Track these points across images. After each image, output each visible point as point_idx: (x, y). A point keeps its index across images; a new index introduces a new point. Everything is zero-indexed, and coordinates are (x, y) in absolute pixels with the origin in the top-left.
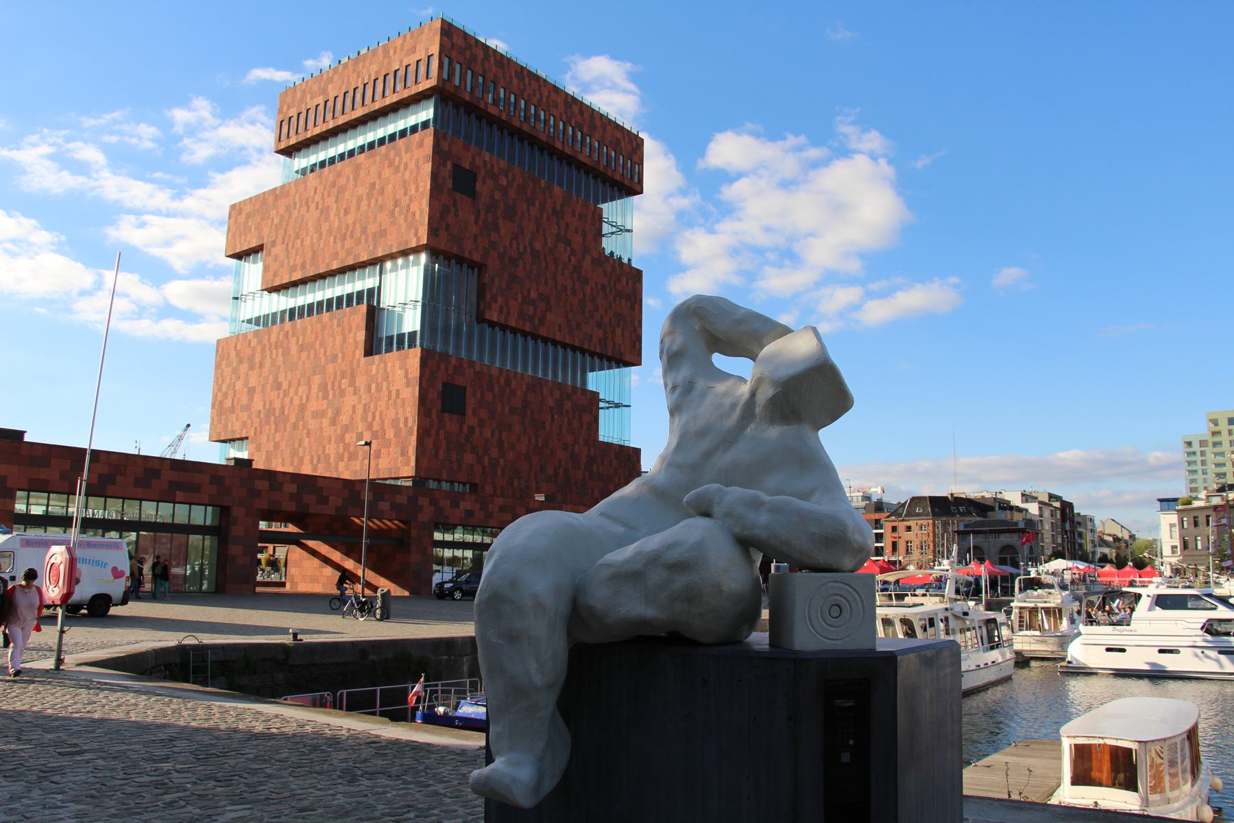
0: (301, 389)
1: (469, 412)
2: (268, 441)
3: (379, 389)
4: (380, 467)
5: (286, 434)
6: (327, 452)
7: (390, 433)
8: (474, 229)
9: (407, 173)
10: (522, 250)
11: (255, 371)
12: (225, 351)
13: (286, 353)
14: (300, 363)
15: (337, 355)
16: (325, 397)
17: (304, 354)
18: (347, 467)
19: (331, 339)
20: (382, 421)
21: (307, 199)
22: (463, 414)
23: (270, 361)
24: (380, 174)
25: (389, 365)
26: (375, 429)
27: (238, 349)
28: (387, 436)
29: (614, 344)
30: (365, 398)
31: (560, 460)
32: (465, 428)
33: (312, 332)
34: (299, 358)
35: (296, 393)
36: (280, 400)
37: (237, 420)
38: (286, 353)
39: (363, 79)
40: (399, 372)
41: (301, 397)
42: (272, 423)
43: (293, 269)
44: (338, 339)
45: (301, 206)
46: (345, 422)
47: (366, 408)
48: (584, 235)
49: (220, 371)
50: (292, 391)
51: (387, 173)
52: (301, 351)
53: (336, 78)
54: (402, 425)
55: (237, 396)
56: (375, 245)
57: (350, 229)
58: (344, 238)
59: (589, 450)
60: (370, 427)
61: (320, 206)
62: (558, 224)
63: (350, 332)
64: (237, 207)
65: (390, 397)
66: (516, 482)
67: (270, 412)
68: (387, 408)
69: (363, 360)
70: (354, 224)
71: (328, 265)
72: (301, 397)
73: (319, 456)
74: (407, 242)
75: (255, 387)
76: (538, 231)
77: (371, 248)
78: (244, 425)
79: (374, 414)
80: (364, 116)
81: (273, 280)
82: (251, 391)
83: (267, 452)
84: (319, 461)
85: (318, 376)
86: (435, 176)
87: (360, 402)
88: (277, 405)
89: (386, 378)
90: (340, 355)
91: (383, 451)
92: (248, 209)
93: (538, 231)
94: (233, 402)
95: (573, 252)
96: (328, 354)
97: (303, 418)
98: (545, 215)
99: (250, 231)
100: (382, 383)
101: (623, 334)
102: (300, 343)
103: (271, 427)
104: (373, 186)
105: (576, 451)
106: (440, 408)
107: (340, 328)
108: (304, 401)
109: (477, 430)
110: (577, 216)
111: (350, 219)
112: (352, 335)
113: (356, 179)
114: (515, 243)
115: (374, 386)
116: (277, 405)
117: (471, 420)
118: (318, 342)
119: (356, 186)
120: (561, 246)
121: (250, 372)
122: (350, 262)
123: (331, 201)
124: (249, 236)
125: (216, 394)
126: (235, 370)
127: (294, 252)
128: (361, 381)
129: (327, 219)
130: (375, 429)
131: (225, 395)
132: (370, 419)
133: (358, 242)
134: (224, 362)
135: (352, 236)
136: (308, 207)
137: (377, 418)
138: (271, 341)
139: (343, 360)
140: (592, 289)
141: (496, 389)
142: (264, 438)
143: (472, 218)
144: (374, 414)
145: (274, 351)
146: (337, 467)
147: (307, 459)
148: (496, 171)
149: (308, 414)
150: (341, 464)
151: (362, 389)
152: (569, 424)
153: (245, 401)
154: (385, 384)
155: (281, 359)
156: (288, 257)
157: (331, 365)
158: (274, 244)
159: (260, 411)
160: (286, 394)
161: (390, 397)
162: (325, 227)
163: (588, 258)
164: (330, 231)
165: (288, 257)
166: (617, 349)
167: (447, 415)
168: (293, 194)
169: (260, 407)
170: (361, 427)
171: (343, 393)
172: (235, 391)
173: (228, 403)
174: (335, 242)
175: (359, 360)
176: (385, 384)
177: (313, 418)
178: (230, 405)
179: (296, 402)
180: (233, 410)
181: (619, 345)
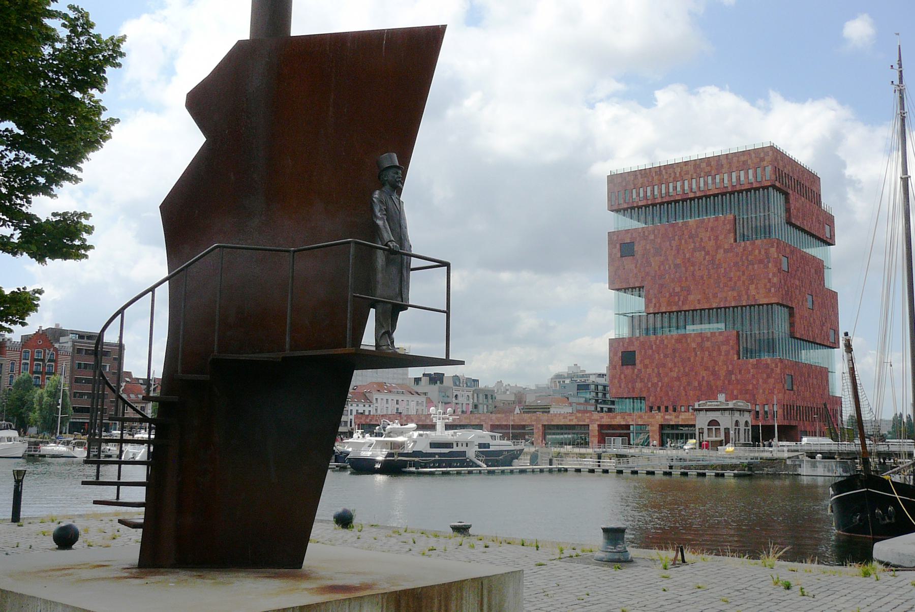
1: (638, 361)
10: (667, 268)
22: (634, 364)
29: (748, 296)
31: (703, 377)
32: (636, 370)
48: (717, 238)
59: (728, 367)
62: (694, 242)
66: (670, 393)
76: (678, 252)
86: (610, 255)
93: (678, 252)
95: (708, 253)
98: (683, 241)
101: (756, 288)
105: (716, 369)
106: (621, 364)
109: (643, 370)
110: (709, 229)
114: (662, 268)
117: (639, 366)
120: (697, 254)
140: (725, 269)
141: (654, 347)
148: (646, 234)
152: (709, 355)
166: (751, 298)
167: (625, 367)
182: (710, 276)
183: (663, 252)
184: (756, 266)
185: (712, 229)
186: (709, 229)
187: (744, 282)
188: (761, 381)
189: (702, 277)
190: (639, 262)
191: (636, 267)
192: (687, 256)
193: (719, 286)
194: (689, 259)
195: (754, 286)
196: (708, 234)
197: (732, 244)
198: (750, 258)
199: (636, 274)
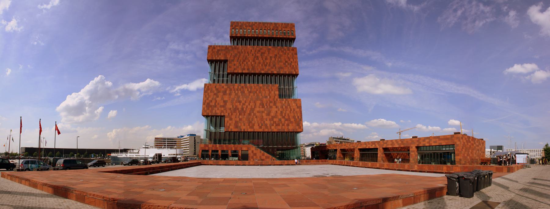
0: (251, 104)
2: (236, 118)
3: (286, 107)
4: (289, 128)
5: (245, 117)
6: (266, 123)
7: (292, 120)
9: (289, 56)
11: (227, 96)
12: (210, 87)
13: (243, 92)
14: (250, 96)
15: (267, 96)
16: (263, 107)
17: (252, 94)
18: (275, 128)
19: (264, 92)
20: (289, 117)
21: (248, 53)
23: (234, 94)
24: (278, 54)
25: (290, 102)
26: (286, 118)
27: (217, 88)
28: (291, 120)
30: (280, 110)
33: (255, 88)
34: (249, 95)
35: (249, 105)
36: (241, 106)
37: (218, 109)
38: (243, 92)
39: (267, 28)
40: (294, 104)
41: (252, 106)
42: (237, 112)
43: (244, 69)
44: (267, 92)
45: (245, 53)
46: (273, 115)
47: (281, 112)
49: (207, 94)
50: (247, 104)
51: (281, 53)
52: (251, 93)
53: (256, 25)
54: (297, 117)
55: (217, 102)
56: (279, 70)
57: (268, 64)
58: (266, 66)
60: (284, 117)
61: (254, 55)
63: (272, 90)
64: (213, 47)
65: (291, 110)
67: (236, 109)
68: (290, 112)
69: (279, 99)
70: (270, 63)
71: (260, 71)
72: (252, 106)
73: (261, 124)
74: (292, 72)
75: (227, 101)
77: (278, 70)
78: (222, 111)
79: (285, 114)
80: (268, 37)
81: (234, 71)
82: (225, 102)
83: (235, 121)
84: (262, 125)
85: (259, 101)
87: (279, 110)
88: (240, 107)
89: (289, 105)
90: (268, 97)
91: (290, 124)
92: (219, 48)
94: (215, 104)
96: (263, 95)
97: (253, 112)
99: (220, 54)
100: (287, 106)
102: (249, 90)
103: (237, 114)
104: (276, 55)
107: (268, 89)
108: (253, 107)
111: (268, 61)
112: (273, 92)
113: (269, 52)
115: (284, 107)
116: (240, 107)
118: (258, 92)
119: (269, 54)
121: (224, 96)
122: (270, 72)
123: (259, 55)
124: (220, 56)
125: (205, 101)
126: (215, 94)
127: (243, 65)
128: (279, 105)
129: (258, 59)
130: (286, 118)
131: (211, 101)
132: (284, 115)
133: (272, 68)
134: (209, 91)
135: (269, 66)
136: (248, 54)
137: (287, 115)
138: (235, 88)
139: (270, 97)
142: (233, 117)
144: (285, 114)
145: (236, 92)
146: (271, 128)
147: (256, 125)
149: (255, 112)
150: (273, 127)
151: (279, 107)
153: (222, 104)
154: (289, 107)
155: (240, 94)
156: (240, 65)
157: (264, 99)
158: (233, 61)
159: (231, 108)
160: (244, 104)
161: (291, 110)
162: (257, 61)
164: (260, 63)
165: (240, 65)
168: (241, 49)
169: (231, 107)
170: (280, 117)
171: (271, 107)
172: (216, 101)
173: (213, 104)
174: (262, 65)
175: (277, 99)
176: (289, 107)
177: (257, 113)
178: (214, 104)
179: (249, 107)
180: (216, 106)
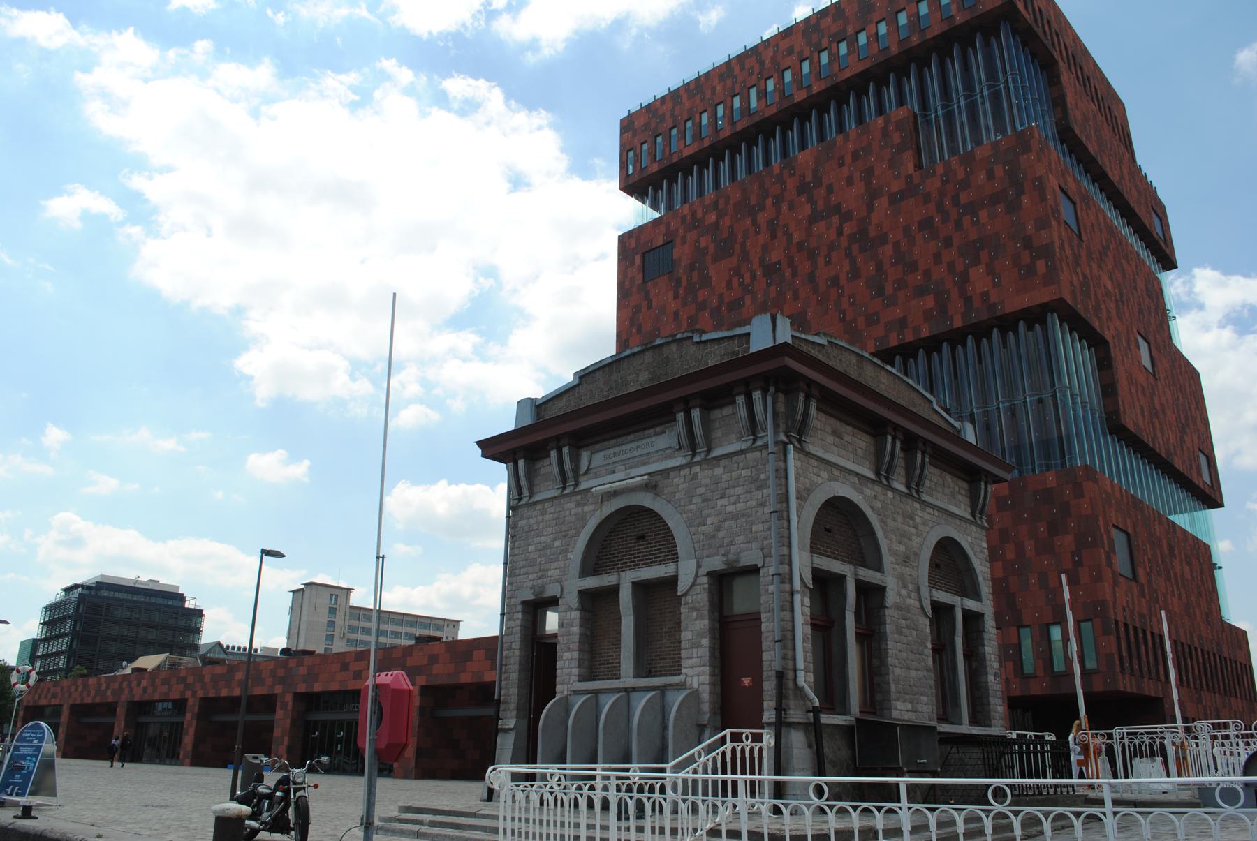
8: (674, 305)
29: (968, 300)
48: (868, 173)
62: (811, 200)
76: (773, 237)
93: (773, 237)
98: (784, 207)
101: (990, 271)
110: (848, 160)
114: (735, 281)
140: (897, 245)
143: (671, 294)
148: (699, 215)
163: (882, 203)
181: (986, 294)
182: (855, 274)
183: (737, 247)
184: (983, 215)
185: (855, 157)
186: (848, 160)
187: (951, 266)
188: (1029, 547)
189: (835, 281)
190: (684, 283)
191: (676, 297)
192: (796, 237)
193: (881, 292)
194: (800, 245)
195: (981, 269)
196: (845, 171)
197: (910, 176)
198: (964, 198)
199: (676, 314)
